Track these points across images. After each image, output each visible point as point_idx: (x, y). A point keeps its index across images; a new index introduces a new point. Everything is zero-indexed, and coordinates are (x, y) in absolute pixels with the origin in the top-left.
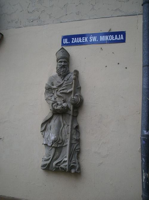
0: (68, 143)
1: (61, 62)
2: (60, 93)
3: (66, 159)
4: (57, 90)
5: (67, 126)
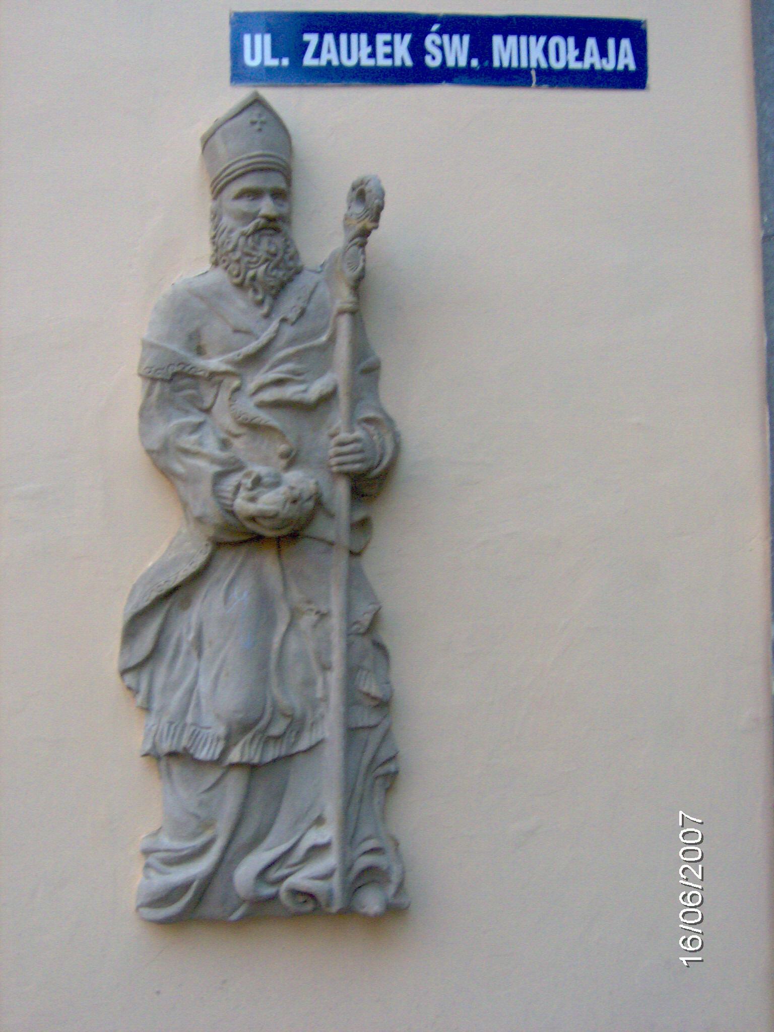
0: (329, 728)
1: (255, 194)
2: (262, 405)
3: (327, 833)
4: (236, 383)
5: (313, 617)
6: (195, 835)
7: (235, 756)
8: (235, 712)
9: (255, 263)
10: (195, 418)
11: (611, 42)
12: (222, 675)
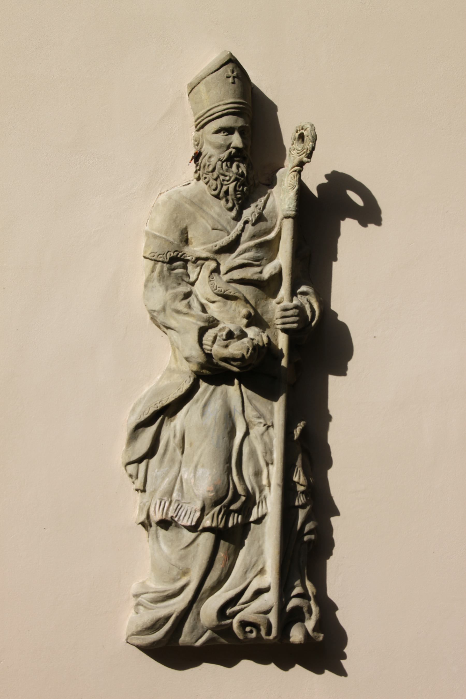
0: (270, 504)
4: (213, 265)
6: (175, 580)
7: (207, 522)
8: (209, 491)
9: (228, 181)
12: (199, 466)
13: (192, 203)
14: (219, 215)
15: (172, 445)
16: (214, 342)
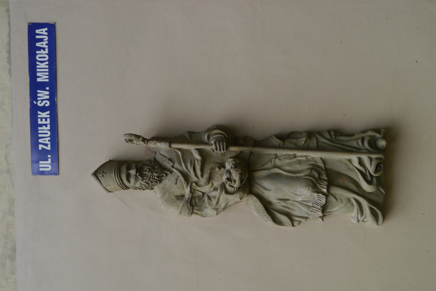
2: (202, 176)
4: (194, 184)
5: (277, 160)
6: (353, 205)
10: (206, 198)
11: (37, 37)
13: (164, 194)
14: (170, 180)
15: (284, 204)
16: (232, 187)
